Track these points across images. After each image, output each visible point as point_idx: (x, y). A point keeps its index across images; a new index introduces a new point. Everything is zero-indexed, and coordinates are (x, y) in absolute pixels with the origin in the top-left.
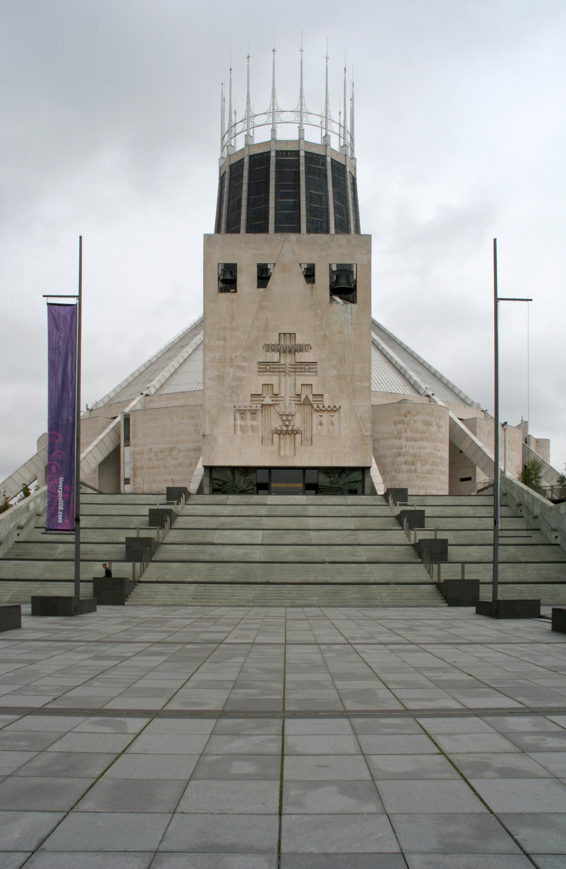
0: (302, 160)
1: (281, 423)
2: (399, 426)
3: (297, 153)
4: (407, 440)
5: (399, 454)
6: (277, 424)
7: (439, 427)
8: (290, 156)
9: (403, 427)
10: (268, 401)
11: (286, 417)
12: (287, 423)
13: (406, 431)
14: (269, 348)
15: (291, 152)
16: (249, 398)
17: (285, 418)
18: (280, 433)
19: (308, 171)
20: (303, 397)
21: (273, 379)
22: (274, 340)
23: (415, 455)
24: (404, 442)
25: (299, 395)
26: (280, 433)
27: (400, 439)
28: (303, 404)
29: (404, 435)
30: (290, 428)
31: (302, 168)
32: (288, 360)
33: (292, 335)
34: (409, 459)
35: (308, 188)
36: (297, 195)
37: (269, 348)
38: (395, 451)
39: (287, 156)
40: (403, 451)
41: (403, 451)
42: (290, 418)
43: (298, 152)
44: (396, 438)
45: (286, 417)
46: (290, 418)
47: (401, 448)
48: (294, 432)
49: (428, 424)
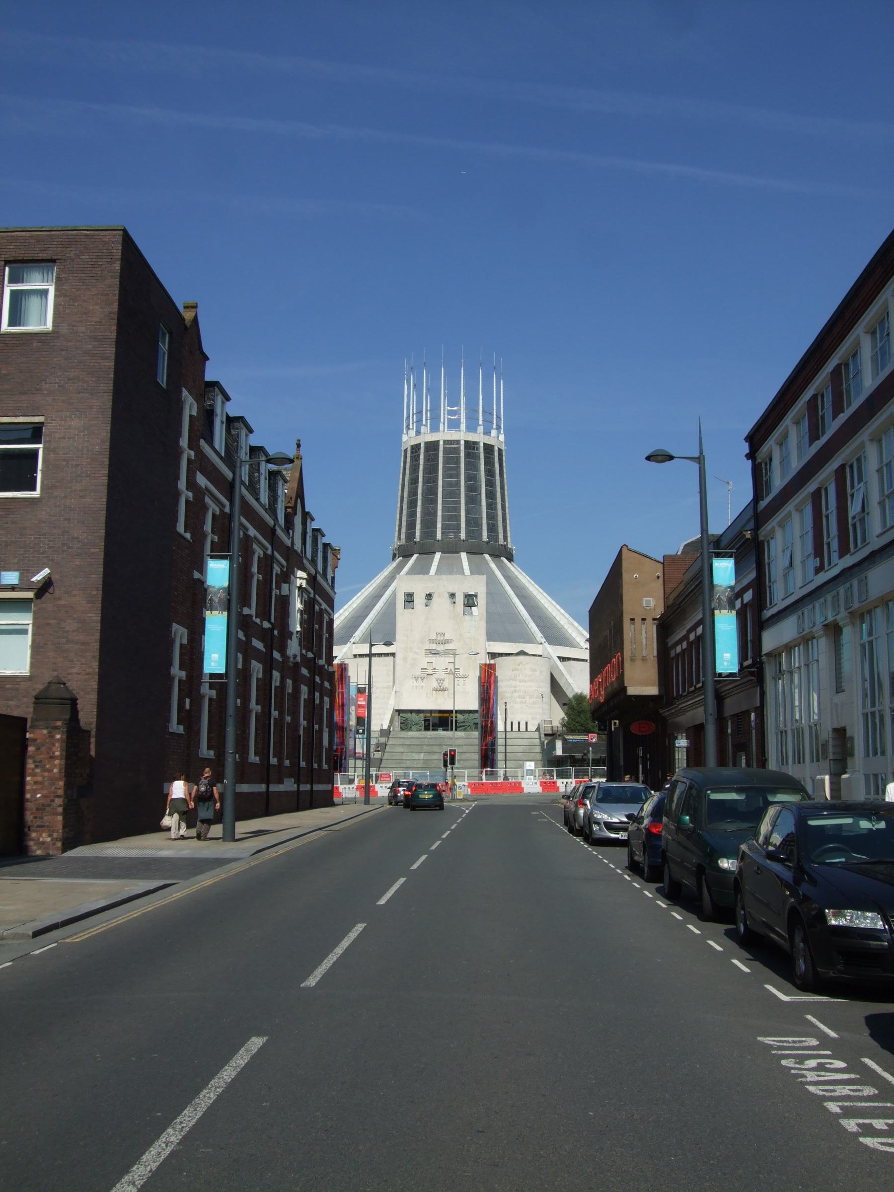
0: (462, 448)
1: (437, 684)
2: (515, 672)
3: (458, 442)
4: (520, 682)
5: (515, 691)
6: (435, 685)
7: (541, 672)
8: (453, 445)
9: (517, 672)
10: (430, 672)
11: (440, 681)
12: (440, 685)
13: (519, 676)
14: (432, 641)
15: (454, 441)
16: (420, 670)
17: (439, 681)
18: (436, 690)
19: (467, 455)
20: (449, 670)
21: (433, 659)
22: (434, 637)
23: (525, 692)
24: (518, 683)
25: (447, 669)
26: (436, 690)
27: (515, 680)
28: (449, 674)
29: (518, 678)
30: (442, 688)
31: (462, 454)
32: (441, 648)
33: (444, 634)
34: (521, 694)
35: (466, 469)
36: (458, 476)
37: (432, 641)
38: (512, 689)
39: (451, 444)
40: (517, 689)
41: (517, 689)
42: (442, 681)
43: (460, 441)
44: (513, 680)
45: (440, 681)
46: (442, 681)
47: (516, 687)
48: (444, 690)
49: (534, 670)
